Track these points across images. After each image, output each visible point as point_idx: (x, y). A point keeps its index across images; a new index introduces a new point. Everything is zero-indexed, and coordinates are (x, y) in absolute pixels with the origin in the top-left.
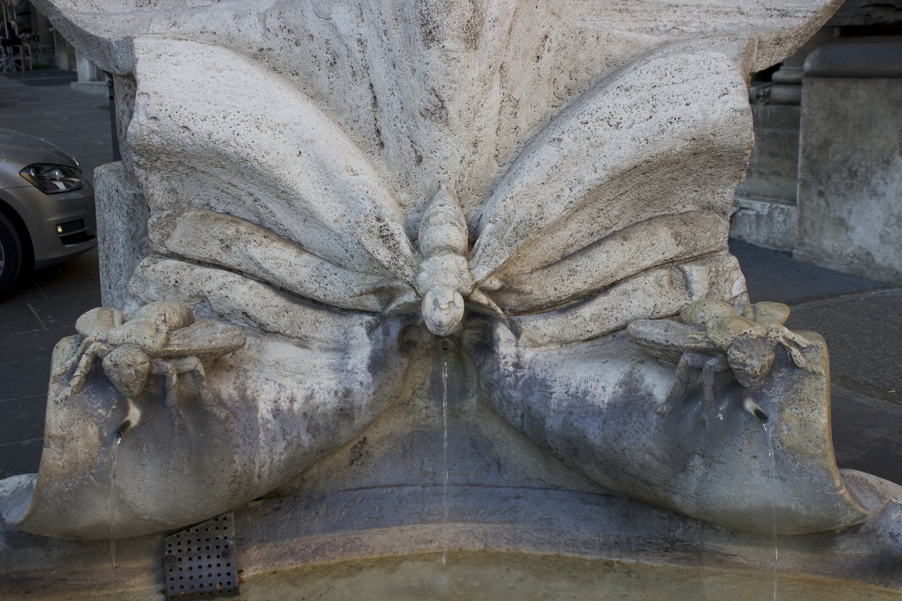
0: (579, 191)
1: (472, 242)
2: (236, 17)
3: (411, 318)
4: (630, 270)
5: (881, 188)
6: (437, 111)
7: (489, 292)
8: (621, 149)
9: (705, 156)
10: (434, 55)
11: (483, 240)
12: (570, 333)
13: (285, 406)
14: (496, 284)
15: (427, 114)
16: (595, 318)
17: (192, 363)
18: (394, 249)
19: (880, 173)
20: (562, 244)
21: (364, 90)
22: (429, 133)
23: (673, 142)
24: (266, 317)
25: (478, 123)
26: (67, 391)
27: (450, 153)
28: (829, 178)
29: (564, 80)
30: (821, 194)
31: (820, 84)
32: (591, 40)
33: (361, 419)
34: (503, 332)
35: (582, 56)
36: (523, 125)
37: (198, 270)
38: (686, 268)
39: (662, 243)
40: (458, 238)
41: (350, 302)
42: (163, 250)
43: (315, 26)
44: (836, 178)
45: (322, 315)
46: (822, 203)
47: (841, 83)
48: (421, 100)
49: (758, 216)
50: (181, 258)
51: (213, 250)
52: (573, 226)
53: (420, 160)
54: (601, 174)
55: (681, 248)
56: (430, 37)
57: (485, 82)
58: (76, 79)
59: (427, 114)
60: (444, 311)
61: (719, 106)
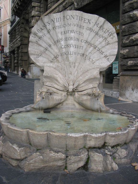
0: (83, 81)
2: (53, 65)
3: (68, 91)
4: (88, 89)
5: (129, 89)
6: (71, 74)
7: (75, 89)
8: (87, 78)
9: (94, 79)
10: (71, 68)
12: (82, 94)
13: (56, 98)
14: (75, 88)
15: (70, 74)
16: (85, 92)
17: (49, 93)
18: (67, 85)
19: (129, 88)
21: (64, 71)
22: (70, 75)
23: (92, 77)
24: (55, 91)
25: (75, 75)
27: (72, 77)
28: (123, 88)
30: (122, 91)
31: (122, 77)
32: (86, 68)
33: (63, 100)
34: (76, 93)
36: (79, 75)
38: (94, 88)
39: (91, 86)
40: (72, 84)
41: (63, 90)
43: (60, 66)
44: (124, 88)
45: (60, 91)
46: (122, 92)
47: (124, 76)
48: (70, 73)
49: (115, 94)
52: (83, 84)
55: (93, 87)
56: (71, 67)
57: (76, 71)
58: (19, 75)
59: (70, 74)
60: (71, 90)
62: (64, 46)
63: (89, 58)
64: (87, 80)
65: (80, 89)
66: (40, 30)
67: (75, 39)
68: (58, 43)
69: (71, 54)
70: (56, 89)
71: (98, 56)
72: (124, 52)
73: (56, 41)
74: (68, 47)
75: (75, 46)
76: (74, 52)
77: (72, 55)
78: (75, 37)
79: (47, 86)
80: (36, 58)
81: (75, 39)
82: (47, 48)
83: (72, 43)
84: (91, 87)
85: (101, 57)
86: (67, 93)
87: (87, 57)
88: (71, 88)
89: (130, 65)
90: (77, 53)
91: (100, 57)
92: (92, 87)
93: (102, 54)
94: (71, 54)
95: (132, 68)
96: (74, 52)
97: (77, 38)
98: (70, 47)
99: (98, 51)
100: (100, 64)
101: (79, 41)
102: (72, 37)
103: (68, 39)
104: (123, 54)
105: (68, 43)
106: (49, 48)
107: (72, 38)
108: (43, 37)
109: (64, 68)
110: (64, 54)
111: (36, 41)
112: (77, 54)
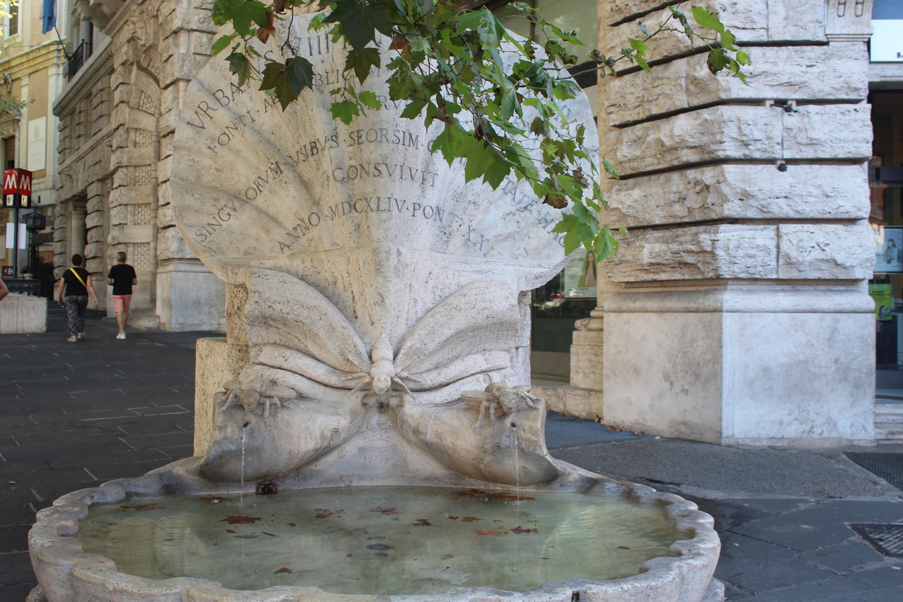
1: (395, 356)
3: (367, 389)
4: (465, 374)
8: (461, 321)
10: (380, 280)
11: (400, 356)
14: (405, 374)
20: (435, 362)
26: (224, 408)
29: (438, 292)
35: (447, 282)
36: (419, 312)
37: (272, 370)
38: (490, 374)
40: (390, 356)
42: (257, 361)
50: (264, 365)
51: (279, 362)
52: (441, 354)
53: (373, 323)
54: (452, 331)
58: (106, 315)
60: (382, 382)
61: (504, 303)
62: (345, 171)
63: (464, 228)
64: (460, 335)
65: (430, 379)
66: (228, 93)
67: (400, 135)
68: (316, 156)
69: (378, 210)
70: (310, 379)
71: (509, 218)
72: (621, 203)
73: (308, 148)
74: (368, 174)
75: (398, 168)
76: (393, 201)
77: (384, 215)
78: (401, 129)
79: (261, 364)
80: (209, 229)
81: (400, 135)
82: (260, 181)
83: (386, 158)
84: (478, 370)
85: (523, 224)
86: (365, 396)
87: (455, 226)
88: (383, 374)
89: (653, 261)
90: (409, 204)
91: (515, 224)
92: (484, 366)
93: (526, 208)
94: (378, 210)
95: (663, 277)
96: (393, 201)
97: (407, 135)
98: (377, 173)
99: (510, 196)
100: (520, 255)
101: (420, 145)
102: (385, 126)
103: (364, 138)
104: (614, 209)
105: (365, 156)
106: (270, 181)
107: (384, 132)
108: (242, 126)
109: (345, 275)
110: (346, 206)
111: (209, 148)
112: (411, 208)
